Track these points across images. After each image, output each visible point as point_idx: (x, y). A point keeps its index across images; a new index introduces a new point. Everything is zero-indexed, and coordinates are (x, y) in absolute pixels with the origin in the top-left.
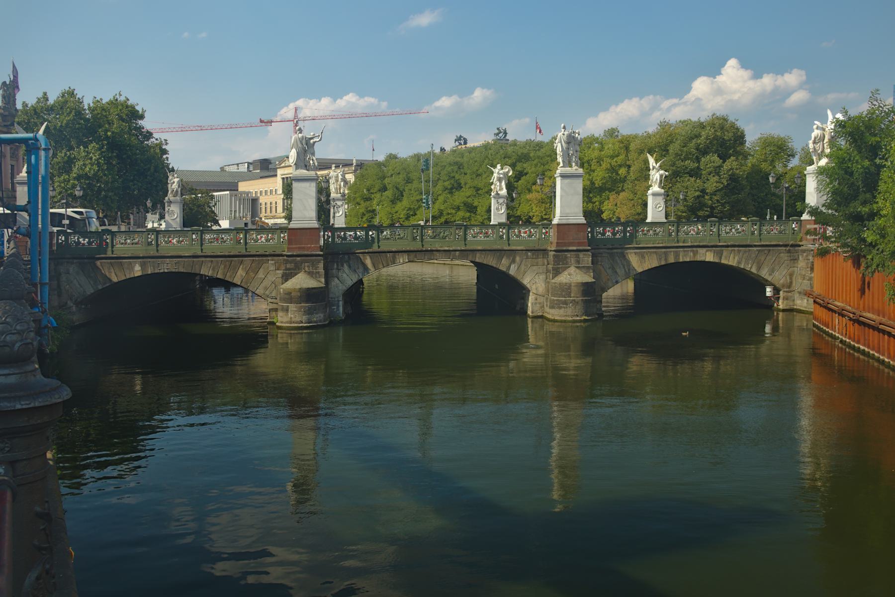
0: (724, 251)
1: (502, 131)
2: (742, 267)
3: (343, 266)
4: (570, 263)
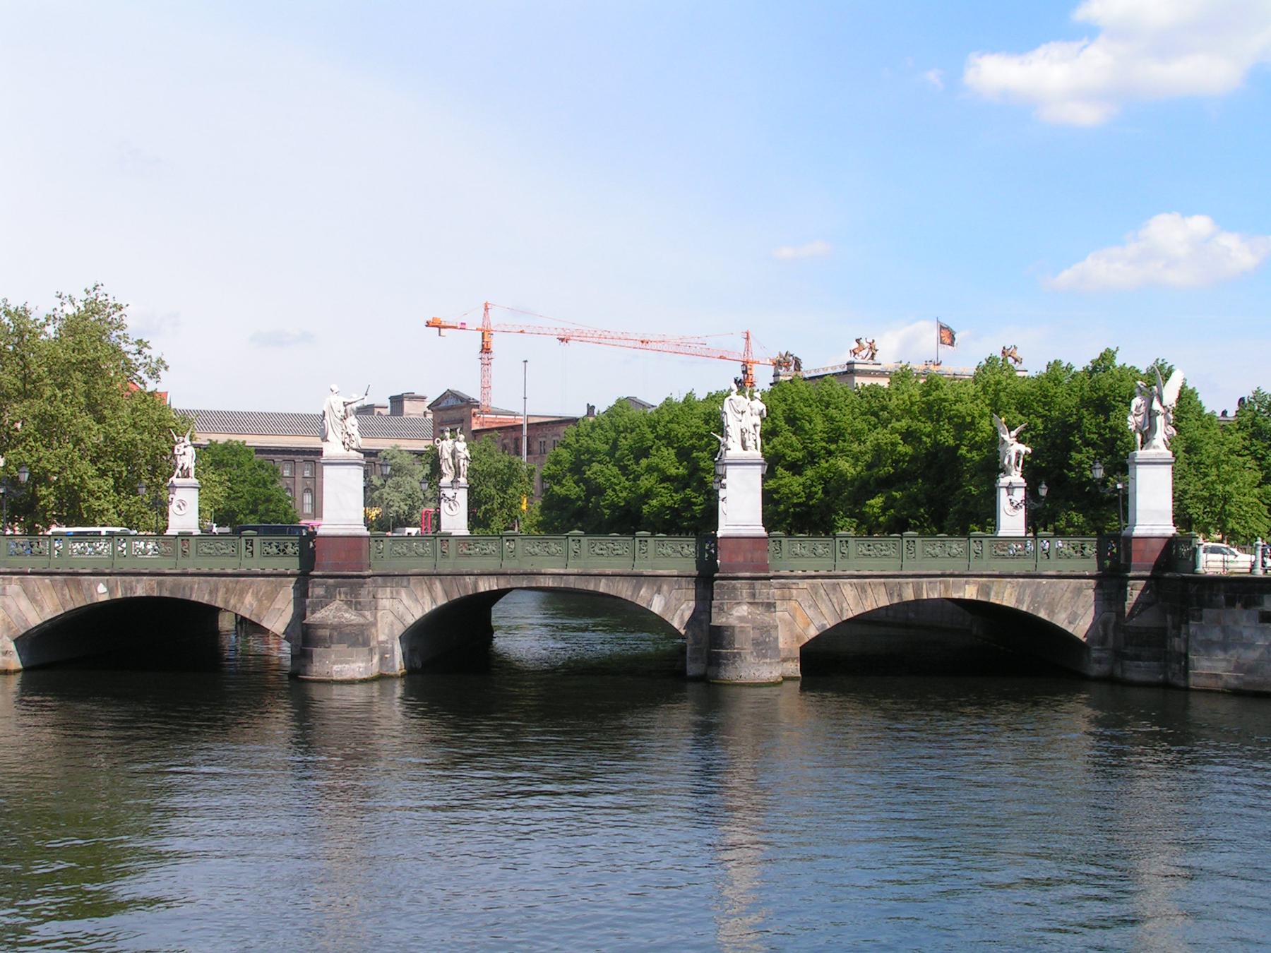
0: (995, 583)
1: (866, 345)
2: (1024, 609)
3: (398, 593)
4: (740, 597)
